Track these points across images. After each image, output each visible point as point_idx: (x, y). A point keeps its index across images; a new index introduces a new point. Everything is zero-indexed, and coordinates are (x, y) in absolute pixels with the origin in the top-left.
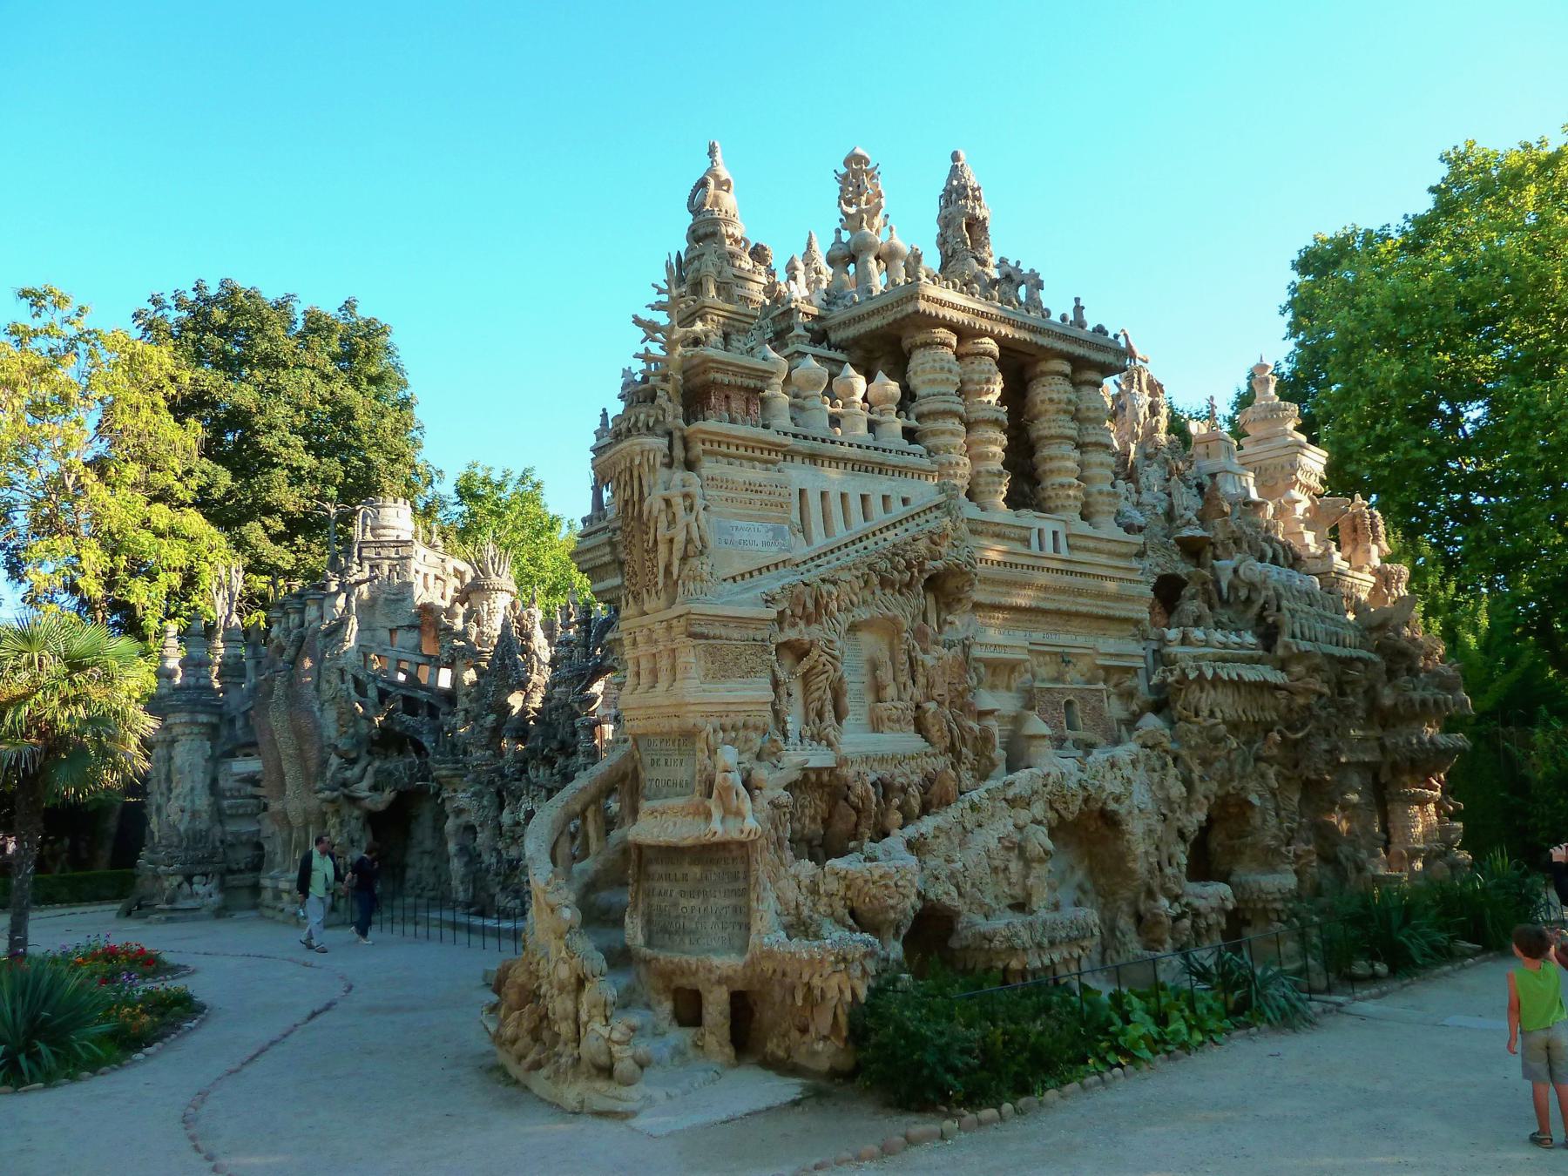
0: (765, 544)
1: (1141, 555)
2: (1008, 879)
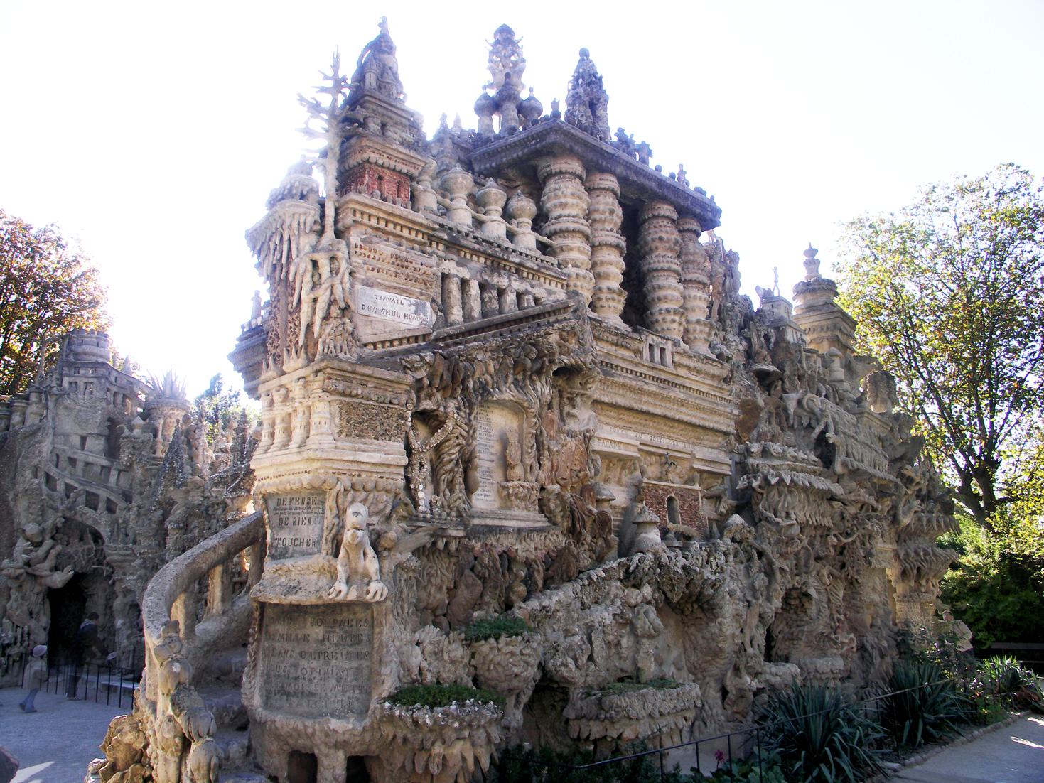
1: (727, 380)
2: (619, 653)
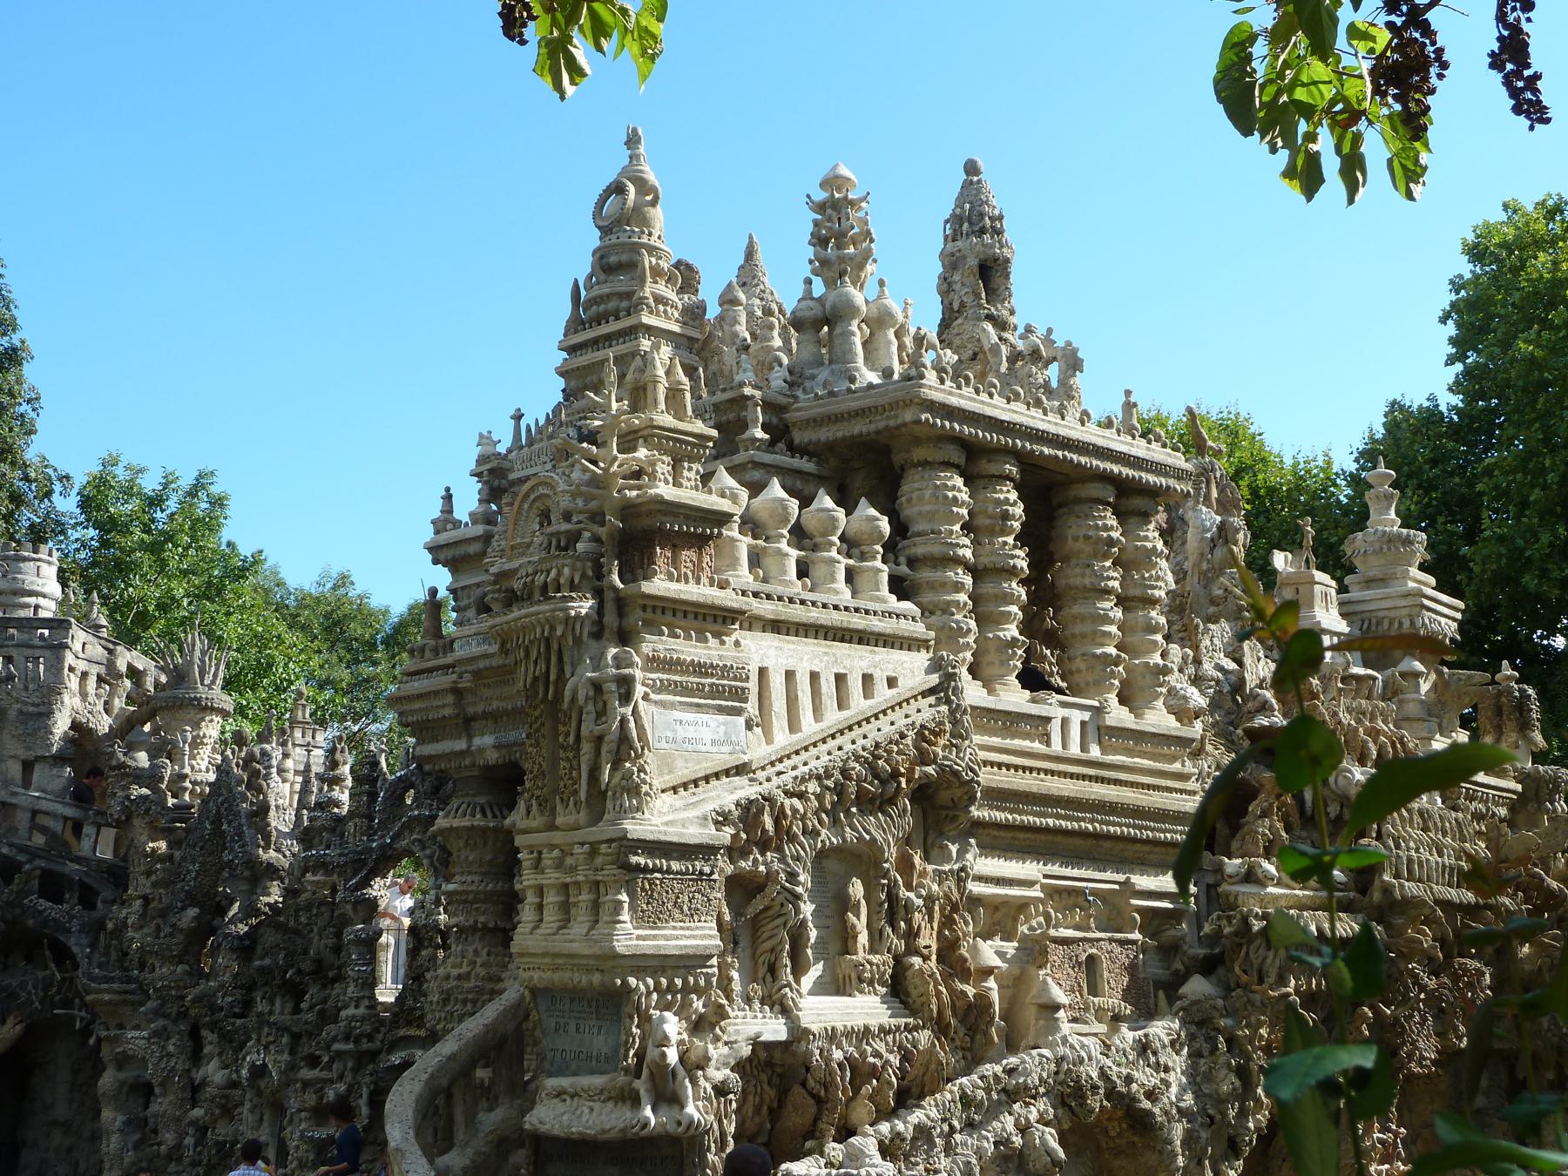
0: (713, 743)
